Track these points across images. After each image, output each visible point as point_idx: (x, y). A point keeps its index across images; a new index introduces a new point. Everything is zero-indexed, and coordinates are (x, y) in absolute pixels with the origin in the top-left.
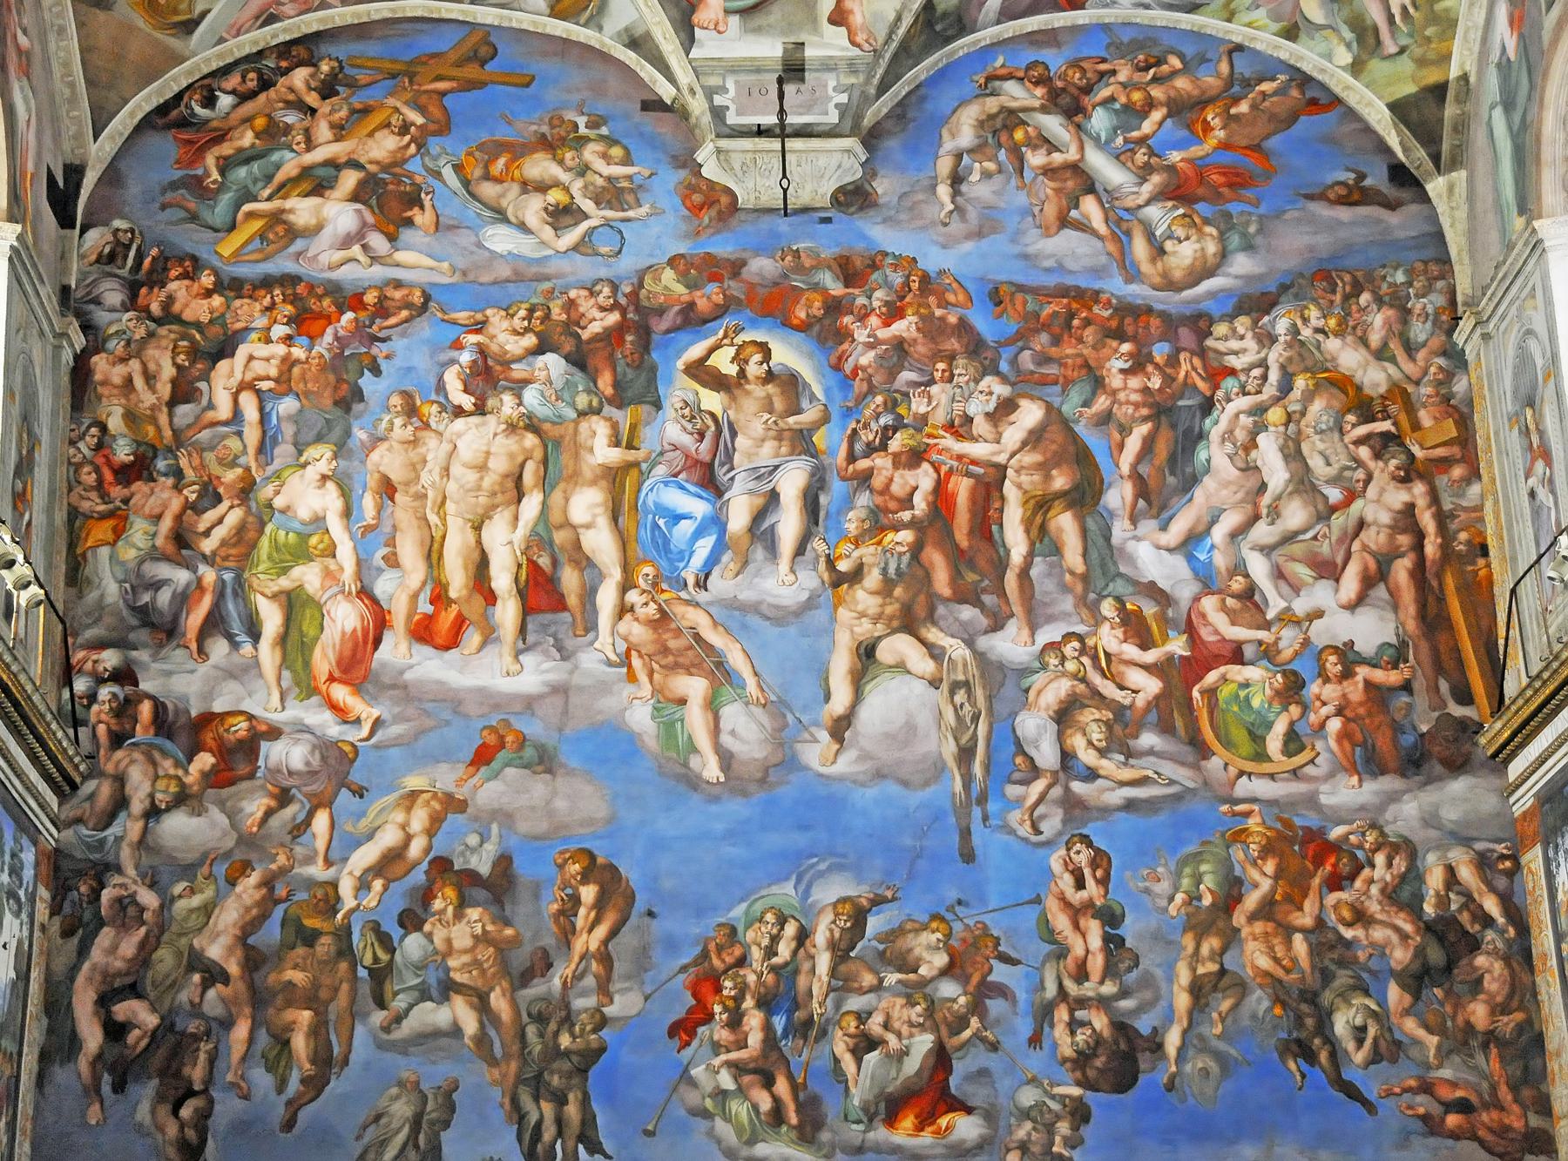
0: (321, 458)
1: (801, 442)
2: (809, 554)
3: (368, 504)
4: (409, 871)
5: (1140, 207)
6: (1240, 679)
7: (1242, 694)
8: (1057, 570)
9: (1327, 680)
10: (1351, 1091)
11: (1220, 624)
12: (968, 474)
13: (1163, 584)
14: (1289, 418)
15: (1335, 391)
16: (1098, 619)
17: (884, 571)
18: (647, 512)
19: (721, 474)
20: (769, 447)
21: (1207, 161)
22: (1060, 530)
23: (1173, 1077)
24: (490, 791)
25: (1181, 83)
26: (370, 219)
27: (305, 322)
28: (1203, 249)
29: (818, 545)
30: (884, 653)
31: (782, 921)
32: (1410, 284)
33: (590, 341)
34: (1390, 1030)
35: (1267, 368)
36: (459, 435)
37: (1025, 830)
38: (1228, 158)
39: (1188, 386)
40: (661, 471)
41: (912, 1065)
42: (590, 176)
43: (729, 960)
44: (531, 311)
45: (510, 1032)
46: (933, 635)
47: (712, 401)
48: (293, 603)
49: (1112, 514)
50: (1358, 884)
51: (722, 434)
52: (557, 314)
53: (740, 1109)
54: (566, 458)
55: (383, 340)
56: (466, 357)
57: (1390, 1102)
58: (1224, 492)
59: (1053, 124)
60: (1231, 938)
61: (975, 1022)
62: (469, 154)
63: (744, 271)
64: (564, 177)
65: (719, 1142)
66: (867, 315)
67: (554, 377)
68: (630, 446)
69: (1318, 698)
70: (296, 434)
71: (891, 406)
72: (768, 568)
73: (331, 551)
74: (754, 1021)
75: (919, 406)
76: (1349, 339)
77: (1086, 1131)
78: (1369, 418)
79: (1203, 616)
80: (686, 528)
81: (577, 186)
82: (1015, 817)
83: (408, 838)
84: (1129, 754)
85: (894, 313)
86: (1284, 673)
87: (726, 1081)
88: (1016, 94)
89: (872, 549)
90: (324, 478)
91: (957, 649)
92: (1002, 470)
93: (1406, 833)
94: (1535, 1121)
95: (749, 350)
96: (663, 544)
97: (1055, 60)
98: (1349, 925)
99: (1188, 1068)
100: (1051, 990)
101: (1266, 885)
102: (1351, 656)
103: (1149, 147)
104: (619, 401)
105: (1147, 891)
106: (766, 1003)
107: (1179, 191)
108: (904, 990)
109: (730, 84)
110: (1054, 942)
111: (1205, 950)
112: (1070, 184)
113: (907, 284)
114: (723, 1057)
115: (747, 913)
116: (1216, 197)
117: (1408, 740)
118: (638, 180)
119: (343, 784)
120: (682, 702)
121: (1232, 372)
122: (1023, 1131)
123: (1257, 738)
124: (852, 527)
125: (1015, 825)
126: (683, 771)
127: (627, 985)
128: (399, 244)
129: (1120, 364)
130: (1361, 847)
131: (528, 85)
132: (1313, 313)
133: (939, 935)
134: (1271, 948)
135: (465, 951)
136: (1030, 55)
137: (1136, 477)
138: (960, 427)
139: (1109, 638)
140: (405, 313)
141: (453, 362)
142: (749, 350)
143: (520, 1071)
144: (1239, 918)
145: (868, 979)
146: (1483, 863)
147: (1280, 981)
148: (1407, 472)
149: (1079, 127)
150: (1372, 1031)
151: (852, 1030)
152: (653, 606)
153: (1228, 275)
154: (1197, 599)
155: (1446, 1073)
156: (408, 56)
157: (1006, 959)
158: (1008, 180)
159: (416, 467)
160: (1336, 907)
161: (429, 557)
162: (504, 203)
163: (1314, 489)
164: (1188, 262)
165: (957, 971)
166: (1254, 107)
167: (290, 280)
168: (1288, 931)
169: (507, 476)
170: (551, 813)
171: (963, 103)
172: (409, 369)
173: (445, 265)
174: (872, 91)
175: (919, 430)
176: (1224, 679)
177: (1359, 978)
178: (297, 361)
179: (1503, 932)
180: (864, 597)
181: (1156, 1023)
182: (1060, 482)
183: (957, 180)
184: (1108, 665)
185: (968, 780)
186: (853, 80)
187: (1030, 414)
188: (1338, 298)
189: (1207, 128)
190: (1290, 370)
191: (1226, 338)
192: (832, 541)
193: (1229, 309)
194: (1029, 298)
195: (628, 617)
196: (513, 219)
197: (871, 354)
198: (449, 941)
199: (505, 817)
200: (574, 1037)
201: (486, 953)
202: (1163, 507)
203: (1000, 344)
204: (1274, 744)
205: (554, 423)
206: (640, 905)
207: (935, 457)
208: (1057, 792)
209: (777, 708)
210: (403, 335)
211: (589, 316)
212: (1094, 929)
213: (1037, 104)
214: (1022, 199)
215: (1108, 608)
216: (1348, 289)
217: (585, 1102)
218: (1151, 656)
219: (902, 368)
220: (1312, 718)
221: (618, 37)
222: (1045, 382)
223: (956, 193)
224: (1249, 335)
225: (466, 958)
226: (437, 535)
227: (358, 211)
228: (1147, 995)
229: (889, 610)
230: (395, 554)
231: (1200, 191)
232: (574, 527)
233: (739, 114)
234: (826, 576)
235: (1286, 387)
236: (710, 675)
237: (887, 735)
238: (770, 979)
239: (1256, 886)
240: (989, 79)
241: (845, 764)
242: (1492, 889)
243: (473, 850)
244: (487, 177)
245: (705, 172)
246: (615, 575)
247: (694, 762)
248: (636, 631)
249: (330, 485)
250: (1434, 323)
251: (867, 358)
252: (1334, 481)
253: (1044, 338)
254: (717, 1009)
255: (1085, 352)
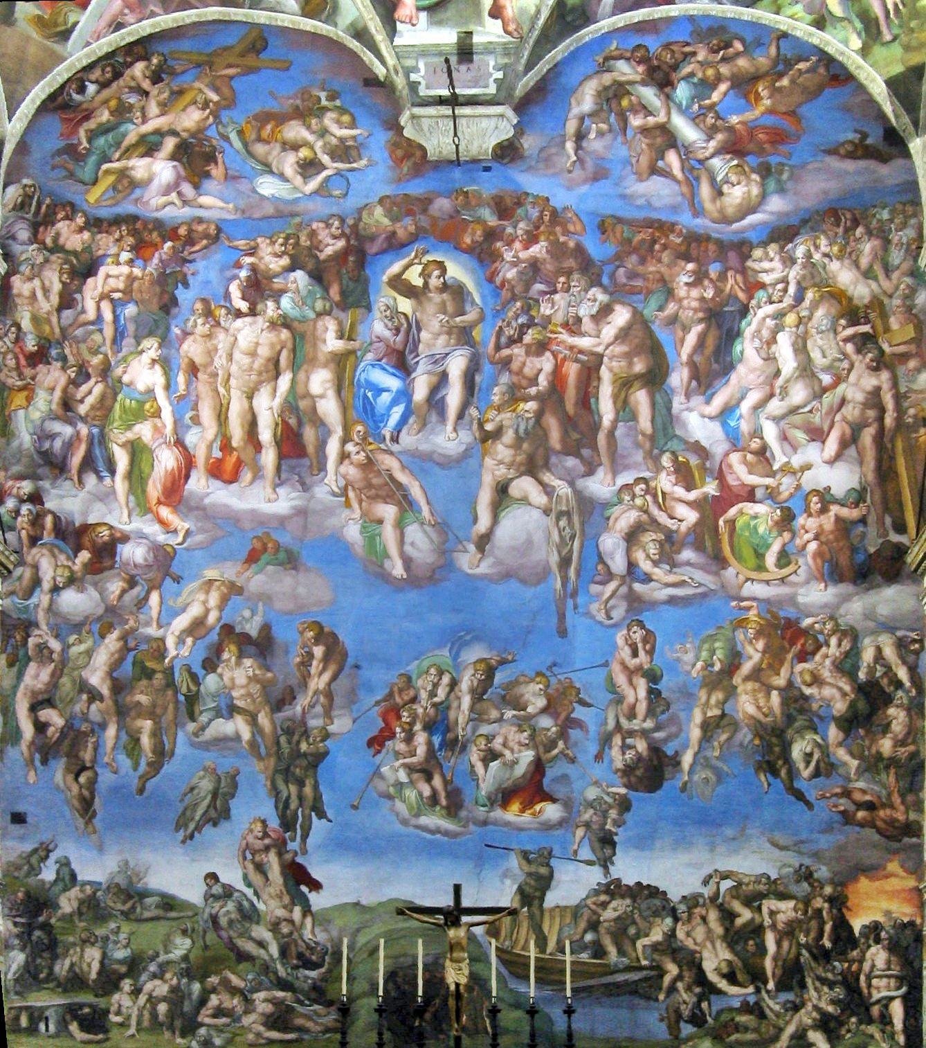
0: (151, 348)
1: (464, 336)
2: (467, 418)
3: (181, 379)
4: (208, 633)
5: (707, 159)
6: (751, 512)
7: (753, 523)
8: (633, 433)
9: (810, 515)
10: (799, 796)
11: (741, 472)
12: (577, 361)
13: (704, 443)
14: (800, 321)
15: (834, 302)
16: (659, 468)
17: (517, 432)
18: (359, 386)
19: (410, 358)
20: (442, 340)
21: (757, 123)
22: (637, 403)
23: (685, 784)
24: (258, 580)
25: (742, 62)
26: (183, 173)
27: (141, 249)
28: (749, 192)
29: (473, 412)
30: (516, 489)
31: (441, 673)
32: (891, 221)
33: (324, 261)
34: (828, 756)
35: (788, 283)
36: (239, 330)
37: (601, 616)
38: (770, 121)
39: (732, 297)
40: (370, 356)
41: (520, 770)
42: (329, 138)
43: (406, 698)
44: (287, 238)
45: (270, 740)
46: (547, 477)
47: (405, 305)
48: (136, 450)
49: (673, 390)
50: (818, 657)
51: (409, 330)
52: (304, 241)
53: (411, 794)
54: (308, 348)
55: (190, 262)
56: (243, 274)
57: (823, 803)
58: (752, 376)
59: (649, 94)
60: (731, 692)
61: (561, 744)
62: (248, 122)
63: (431, 207)
64: (310, 138)
65: (397, 814)
66: (513, 241)
67: (301, 287)
68: (350, 339)
69: (803, 527)
70: (137, 330)
71: (527, 309)
72: (439, 428)
73: (157, 414)
74: (421, 738)
75: (546, 309)
76: (847, 262)
77: (628, 817)
78: (854, 322)
79: (730, 467)
80: (385, 398)
81: (319, 145)
82: (594, 607)
83: (207, 611)
84: (674, 565)
85: (531, 239)
86: (782, 509)
87: (403, 776)
88: (625, 70)
89: (509, 415)
90: (154, 361)
91: (563, 489)
92: (601, 356)
93: (852, 622)
94: (913, 816)
95: (432, 267)
96: (368, 408)
97: (653, 44)
98: (809, 685)
99: (696, 778)
100: (611, 724)
101: (757, 657)
102: (828, 498)
103: (716, 112)
104: (344, 305)
105: (678, 660)
106: (429, 727)
107: (735, 147)
108: (516, 721)
109: (421, 65)
110: (615, 693)
111: (713, 701)
112: (659, 140)
113: (541, 217)
114: (401, 761)
115: (418, 666)
116: (761, 152)
117: (861, 557)
118: (360, 139)
119: (167, 574)
120: (380, 522)
121: (763, 286)
122: (588, 815)
123: (760, 556)
124: (496, 399)
125: (595, 613)
126: (379, 570)
127: (342, 712)
128: (202, 191)
129: (685, 279)
130: (821, 632)
131: (287, 69)
132: (823, 241)
133: (541, 686)
134: (756, 700)
135: (242, 687)
136: (637, 40)
137: (692, 364)
138: (573, 325)
139: (665, 482)
140: (205, 242)
141: (236, 277)
142: (432, 267)
143: (276, 765)
144: (737, 680)
145: (494, 714)
146: (901, 645)
147: (759, 722)
148: (878, 364)
149: (668, 97)
150: (816, 756)
151: (483, 747)
152: (363, 454)
153: (764, 212)
154: (727, 454)
155: (861, 784)
156: (210, 50)
157: (583, 703)
158: (615, 139)
159: (211, 353)
160: (801, 673)
161: (219, 416)
162: (270, 159)
163: (813, 375)
164: (738, 201)
165: (552, 710)
166: (793, 82)
167: (132, 219)
168: (768, 689)
169: (269, 360)
170: (295, 597)
171: (588, 78)
172: (208, 282)
173: (231, 206)
174: (521, 68)
175: (545, 328)
176: (741, 513)
177: (811, 720)
178: (136, 278)
179: (908, 692)
180: (502, 450)
181: (678, 748)
182: (639, 367)
183: (580, 137)
184: (663, 501)
185: (565, 580)
186: (506, 61)
187: (621, 316)
188: (841, 230)
189: (758, 98)
190: (804, 285)
191: (760, 260)
192: (483, 409)
193: (764, 237)
194: (625, 228)
195: (346, 462)
196: (275, 170)
197: (515, 270)
198: (232, 679)
199: (266, 598)
200: (309, 744)
201: (255, 689)
202: (709, 386)
203: (603, 263)
204: (771, 559)
205: (300, 322)
206: (351, 661)
207: (554, 348)
208: (624, 590)
209: (442, 527)
210: (203, 258)
211: (325, 242)
212: (642, 685)
213: (638, 78)
214: (623, 152)
215: (666, 460)
216: (849, 223)
217: (316, 787)
218: (693, 495)
219: (535, 282)
220: (798, 542)
221: (346, 31)
222: (634, 291)
223: (578, 147)
224: (777, 258)
225: (243, 691)
226: (224, 402)
227: (174, 167)
228: (674, 729)
229: (519, 459)
230: (198, 416)
231: (751, 147)
232: (313, 397)
233: (428, 87)
234: (477, 434)
235: (799, 299)
236: (399, 504)
237: (513, 548)
238: (431, 711)
239: (750, 658)
240: (607, 59)
241: (484, 568)
242: (904, 662)
243: (247, 621)
244: (259, 139)
245: (406, 133)
246: (338, 432)
247: (387, 564)
248: (352, 471)
249: (157, 367)
250: (907, 250)
251: (511, 274)
252: (827, 369)
253: (634, 258)
254: (398, 730)
255: (663, 269)
